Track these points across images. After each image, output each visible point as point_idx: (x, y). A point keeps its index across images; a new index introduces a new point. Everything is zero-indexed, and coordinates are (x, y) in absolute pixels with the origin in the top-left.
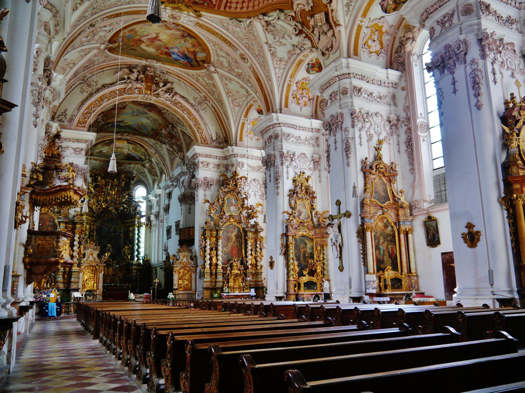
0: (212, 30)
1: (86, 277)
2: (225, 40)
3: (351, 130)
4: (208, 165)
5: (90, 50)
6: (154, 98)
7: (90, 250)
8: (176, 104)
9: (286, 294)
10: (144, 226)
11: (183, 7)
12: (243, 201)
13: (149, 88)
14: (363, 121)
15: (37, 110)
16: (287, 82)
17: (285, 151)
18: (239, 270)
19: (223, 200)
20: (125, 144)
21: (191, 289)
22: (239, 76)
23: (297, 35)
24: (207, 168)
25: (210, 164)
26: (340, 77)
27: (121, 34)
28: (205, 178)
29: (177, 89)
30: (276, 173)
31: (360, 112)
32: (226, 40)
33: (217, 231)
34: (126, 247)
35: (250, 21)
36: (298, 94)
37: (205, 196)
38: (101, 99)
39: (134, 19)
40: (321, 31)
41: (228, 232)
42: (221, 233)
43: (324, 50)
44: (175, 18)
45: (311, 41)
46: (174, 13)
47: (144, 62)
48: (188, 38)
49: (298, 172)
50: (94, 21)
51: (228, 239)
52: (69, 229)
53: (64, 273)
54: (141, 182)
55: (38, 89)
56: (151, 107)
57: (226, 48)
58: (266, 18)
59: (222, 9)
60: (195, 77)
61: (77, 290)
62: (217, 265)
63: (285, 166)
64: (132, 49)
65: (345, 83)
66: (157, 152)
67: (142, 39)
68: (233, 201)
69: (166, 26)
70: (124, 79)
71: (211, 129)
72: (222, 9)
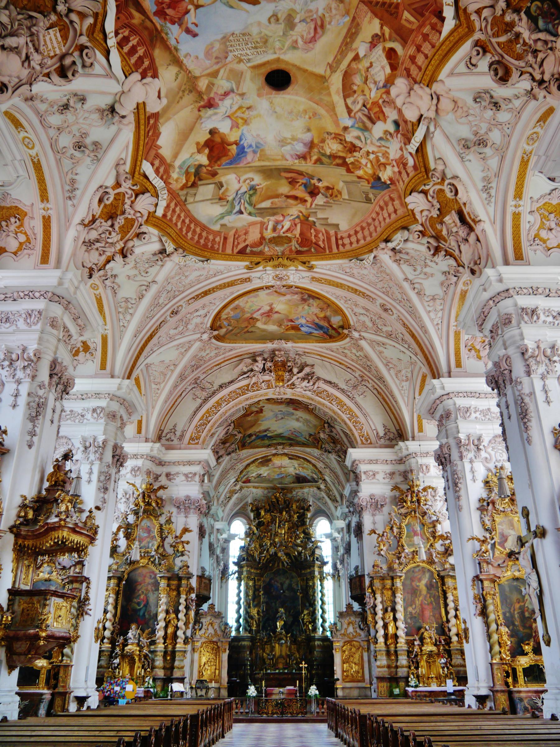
1: (204, 660)
2: (355, 291)
3: (525, 380)
4: (374, 475)
5: (190, 344)
6: (289, 391)
7: (209, 618)
8: (318, 393)
9: (493, 691)
10: (329, 578)
11: (285, 262)
12: (434, 526)
13: (279, 379)
14: (547, 361)
15: (34, 426)
16: (452, 329)
17: (462, 436)
18: (435, 645)
19: (400, 528)
20: (285, 461)
21: (363, 680)
22: (389, 336)
23: (434, 255)
24: (374, 481)
25: (378, 473)
26: (496, 298)
27: (224, 316)
28: (372, 497)
29: (319, 372)
30: (454, 473)
31: (538, 347)
32: (356, 290)
33: (392, 578)
34: (306, 612)
35: (372, 255)
36: (476, 344)
37: (374, 523)
38: (219, 404)
39: (232, 293)
40: (460, 239)
41: (412, 580)
42: (398, 583)
43: (471, 265)
44: (281, 279)
45: (455, 258)
47: (269, 346)
48: (311, 301)
49: (491, 466)
50: (175, 307)
51: (413, 592)
52: (173, 587)
53: (165, 653)
54: (321, 513)
55: (37, 399)
56: (293, 403)
57: (361, 301)
59: (335, 250)
60: (341, 350)
61: (181, 680)
62: (396, 637)
63: (466, 461)
64: (248, 332)
65: (506, 306)
66: (327, 466)
67: (254, 316)
68: (418, 528)
70: (245, 373)
71: (375, 421)
72: (335, 250)
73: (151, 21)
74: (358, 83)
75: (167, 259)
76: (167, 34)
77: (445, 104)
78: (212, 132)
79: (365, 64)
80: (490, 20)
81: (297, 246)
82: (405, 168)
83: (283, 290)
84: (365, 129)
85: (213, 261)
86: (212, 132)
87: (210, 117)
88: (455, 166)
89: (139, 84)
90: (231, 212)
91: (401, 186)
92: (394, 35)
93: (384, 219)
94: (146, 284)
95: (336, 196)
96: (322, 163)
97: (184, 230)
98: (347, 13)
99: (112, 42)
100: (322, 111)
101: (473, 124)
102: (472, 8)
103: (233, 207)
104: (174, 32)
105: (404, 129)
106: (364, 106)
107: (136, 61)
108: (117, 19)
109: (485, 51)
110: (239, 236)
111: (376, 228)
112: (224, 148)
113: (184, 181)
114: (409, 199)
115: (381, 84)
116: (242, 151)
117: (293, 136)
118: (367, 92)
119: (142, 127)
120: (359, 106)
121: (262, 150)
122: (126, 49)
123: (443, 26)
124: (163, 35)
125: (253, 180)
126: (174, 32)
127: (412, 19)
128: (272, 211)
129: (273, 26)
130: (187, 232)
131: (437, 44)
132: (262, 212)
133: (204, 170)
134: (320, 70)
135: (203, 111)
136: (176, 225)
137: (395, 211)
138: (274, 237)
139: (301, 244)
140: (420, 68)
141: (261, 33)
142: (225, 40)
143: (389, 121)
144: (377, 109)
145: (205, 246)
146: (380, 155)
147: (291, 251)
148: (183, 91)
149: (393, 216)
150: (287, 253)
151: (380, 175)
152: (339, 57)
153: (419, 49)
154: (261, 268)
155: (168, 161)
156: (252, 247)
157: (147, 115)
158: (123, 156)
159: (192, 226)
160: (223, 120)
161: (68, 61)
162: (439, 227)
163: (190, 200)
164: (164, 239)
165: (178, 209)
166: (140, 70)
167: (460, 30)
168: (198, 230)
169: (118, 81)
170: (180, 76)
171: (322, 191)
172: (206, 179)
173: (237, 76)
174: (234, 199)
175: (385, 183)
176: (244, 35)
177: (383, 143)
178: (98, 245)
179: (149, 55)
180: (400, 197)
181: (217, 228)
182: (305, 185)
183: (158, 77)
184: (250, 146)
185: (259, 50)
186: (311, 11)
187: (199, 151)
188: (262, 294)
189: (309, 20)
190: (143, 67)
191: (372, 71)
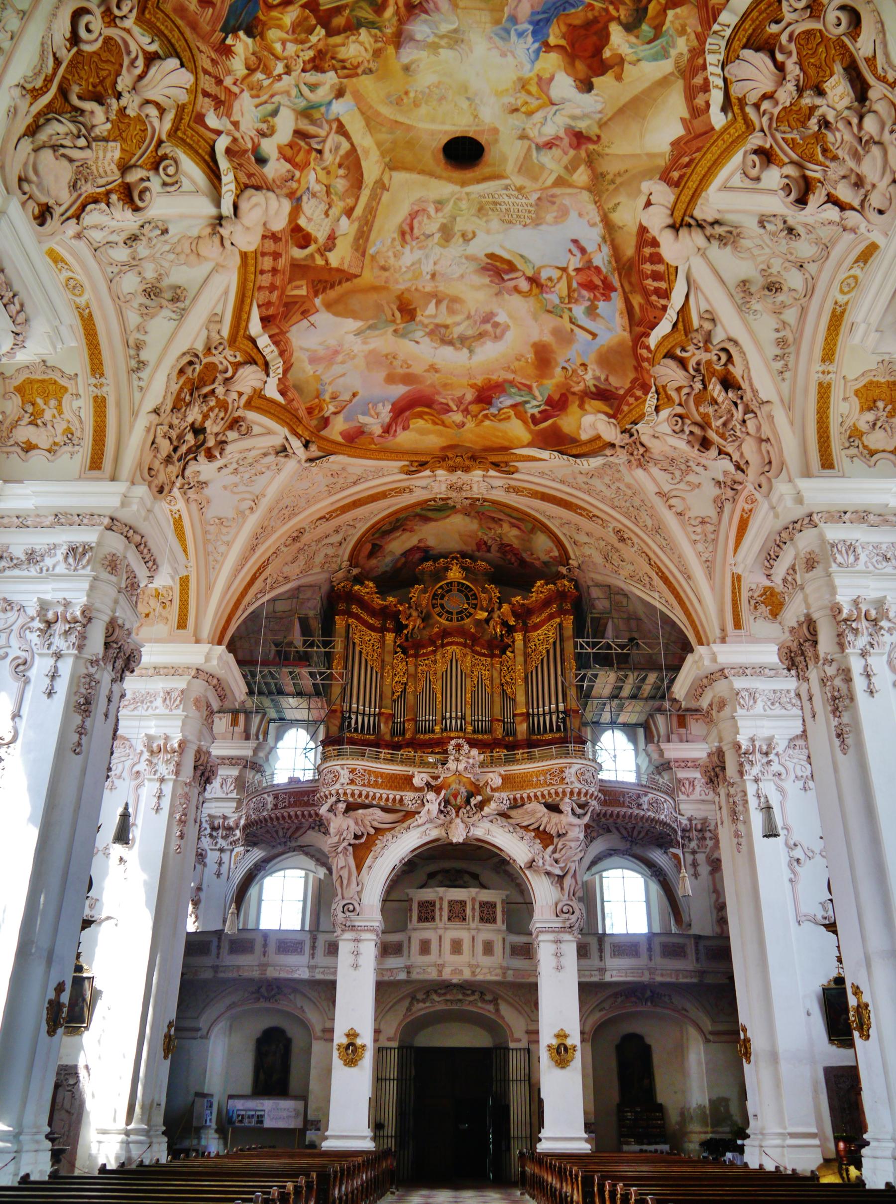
73: (622, 286)
74: (338, 180)
76: (610, 262)
78: (587, 86)
87: (585, 116)
92: (309, 262)
98: (373, 257)
99: (671, 315)
100: (387, 111)
106: (320, 152)
112: (572, 44)
113: (671, 13)
115: (305, 198)
118: (322, 175)
121: (497, 22)
126: (601, 258)
129: (469, 228)
131: (256, 294)
133: (623, 13)
134: (399, 177)
135: (595, 131)
141: (487, 222)
142: (537, 222)
144: (298, 159)
146: (266, 83)
151: (250, 41)
152: (374, 204)
155: (680, 84)
157: (677, 190)
170: (611, 205)
173: (526, 167)
175: (234, 31)
176: (510, 222)
177: (269, 107)
184: (520, 35)
185: (491, 200)
186: (420, 248)
189: (422, 237)
191: (323, 207)
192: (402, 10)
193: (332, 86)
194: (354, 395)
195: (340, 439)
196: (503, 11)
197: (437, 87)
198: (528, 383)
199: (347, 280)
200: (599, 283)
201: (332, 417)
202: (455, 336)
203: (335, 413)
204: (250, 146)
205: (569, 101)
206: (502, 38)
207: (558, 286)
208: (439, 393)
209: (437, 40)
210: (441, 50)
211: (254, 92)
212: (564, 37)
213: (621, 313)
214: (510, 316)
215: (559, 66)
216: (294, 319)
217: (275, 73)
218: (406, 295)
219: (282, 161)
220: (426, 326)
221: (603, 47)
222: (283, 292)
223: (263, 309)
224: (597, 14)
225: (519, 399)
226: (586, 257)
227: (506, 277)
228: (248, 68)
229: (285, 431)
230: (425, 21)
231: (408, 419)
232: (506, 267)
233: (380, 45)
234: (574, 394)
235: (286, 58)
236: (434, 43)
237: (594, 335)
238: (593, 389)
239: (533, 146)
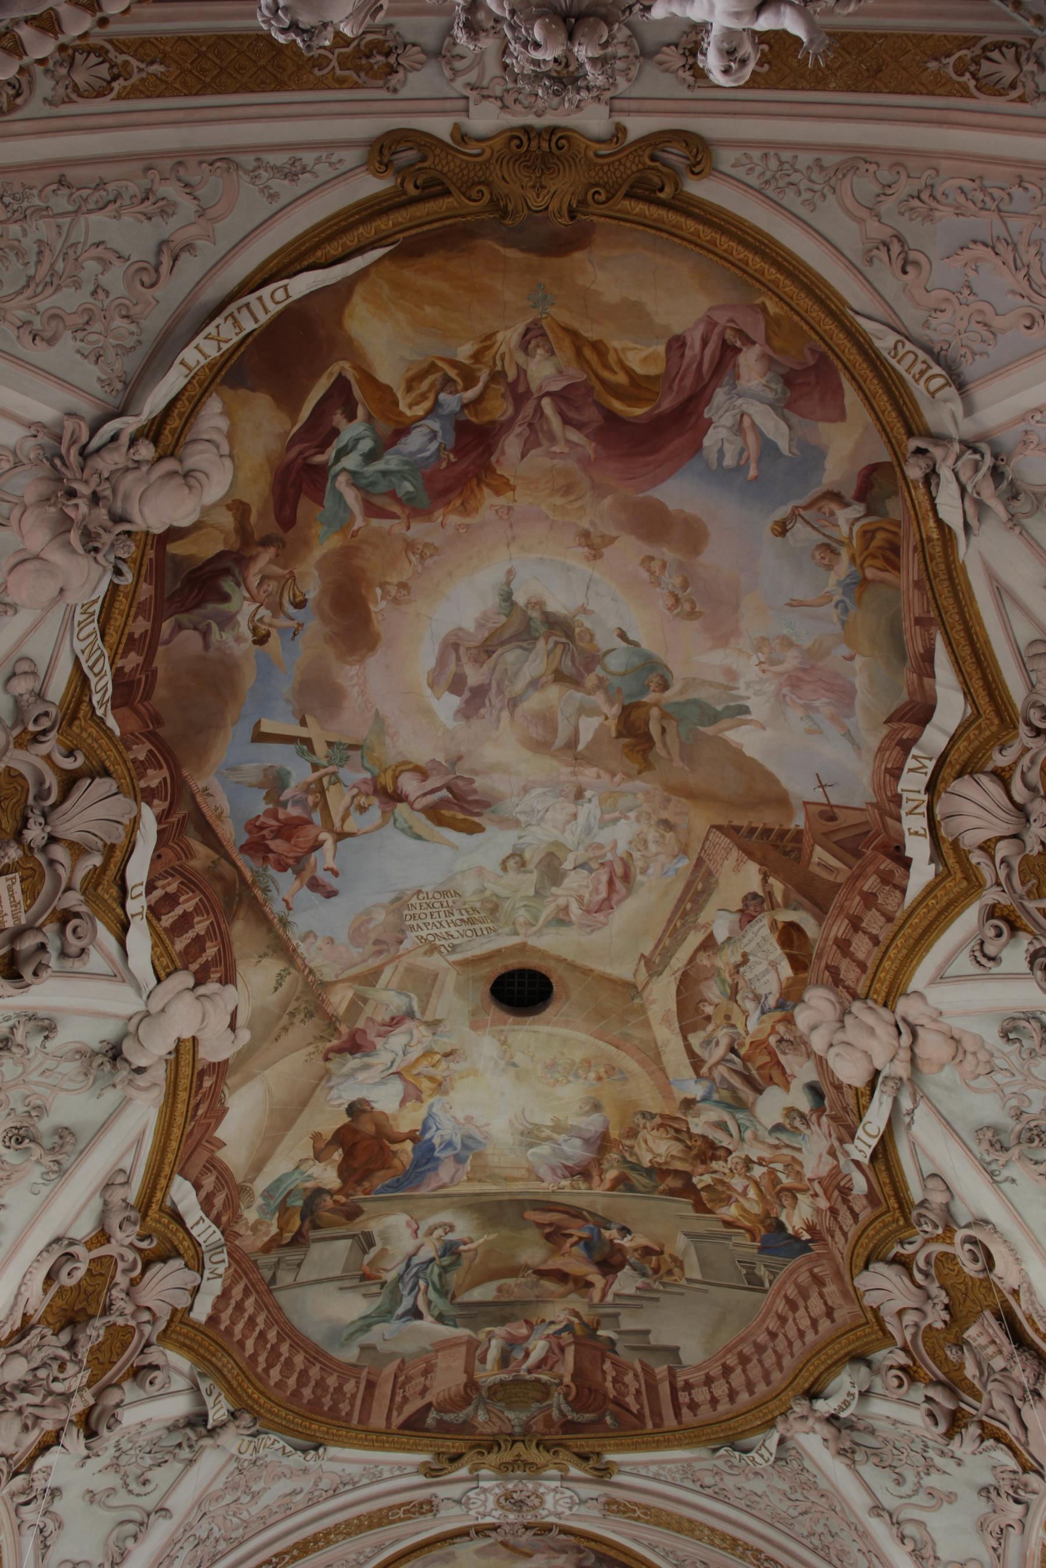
0: (669, 1514)
11: (534, 1455)
32: (735, 1540)
39: (380, 1548)
40: (1017, 1392)
44: (519, 1505)
46: (510, 1486)
58: (824, 1407)
59: (670, 1422)
69: (504, 1544)
72: (670, 1422)
73: (234, 864)
74: (716, 1000)
75: (207, 1442)
76: (266, 890)
77: (931, 1046)
79: (730, 957)
80: (1015, 863)
81: (565, 1408)
82: (845, 1201)
83: (526, 1538)
84: (737, 1105)
85: (333, 1451)
86: (355, 1109)
87: (351, 1074)
88: (975, 1194)
89: (189, 997)
90: (390, 1312)
91: (840, 1246)
92: (795, 896)
93: (801, 1334)
94: (137, 1515)
95: (670, 1272)
96: (631, 1188)
97: (262, 1359)
98: (684, 851)
99: (137, 905)
100: (630, 1064)
101: (1008, 1090)
102: (971, 840)
103: (396, 1298)
104: (283, 887)
105: (836, 1105)
107: (188, 946)
108: (157, 857)
109: (1014, 928)
110: (409, 1379)
111: (779, 1357)
112: (383, 1148)
113: (274, 1230)
114: (864, 1280)
115: (772, 1002)
116: (426, 1157)
117: (555, 1120)
118: (737, 1019)
119: (183, 1095)
120: (720, 1051)
121: (478, 1155)
122: (167, 920)
123: (908, 877)
124: (258, 892)
125: (452, 1228)
126: (283, 887)
127: (834, 862)
128: (500, 1311)
129: (513, 877)
130: (270, 1365)
132: (474, 1314)
133: (329, 1202)
134: (623, 971)
135: (336, 1059)
136: (241, 1344)
137: (829, 1313)
138: (502, 1383)
139: (577, 1404)
140: (862, 966)
141: (483, 890)
142: (400, 903)
143: (797, 1086)
144: (766, 1059)
145: (315, 1405)
147: (548, 1421)
148: (292, 1015)
149: (824, 1325)
150: (538, 1427)
151: (783, 1218)
152: (667, 942)
153: (856, 924)
154: (463, 1472)
155: (239, 1179)
156: (441, 1409)
157: (199, 1067)
158: (126, 1164)
159: (285, 1348)
160: (383, 1081)
161: (27, 944)
162: (952, 1355)
163: (286, 1278)
164: (204, 1385)
165: (250, 1303)
166: (194, 967)
167: (948, 884)
168: (299, 1360)
169: (138, 989)
170: (288, 979)
171: (632, 1258)
172: (332, 1224)
173: (426, 983)
174: (400, 1278)
175: (796, 1238)
176: (444, 893)
177: (785, 1138)
178: (25, 1399)
179: (219, 934)
180: (838, 1275)
181: (350, 1355)
182: (588, 1244)
183: (235, 984)
184: (449, 1144)
185: (477, 927)
186: (600, 846)
187: (319, 1156)
188: (465, 1550)
189: (594, 865)
190: (202, 960)
191: (749, 973)
192: (595, 1173)
193: (697, 1115)
194: (782, 529)
195: (851, 396)
196: (472, 1166)
197: (557, 1081)
198: (375, 522)
199: (737, 829)
200: (272, 844)
201: (849, 491)
202: (541, 644)
203: (835, 496)
204: (824, 1119)
205: (375, 1084)
206: (471, 1137)
207: (347, 799)
208: (585, 463)
209: (555, 1136)
210: (550, 1123)
211: (797, 1168)
212: (394, 1153)
213: (219, 817)
214: (429, 713)
215: (395, 1120)
216: (854, 818)
217: (765, 1169)
218: (636, 767)
219: (788, 1071)
220: (601, 684)
221: (344, 1160)
222: (855, 878)
223: (897, 880)
224: (360, 1189)
225: (391, 461)
226: (307, 876)
227: (444, 793)
228: (795, 1198)
229: (966, 552)
230: (568, 1158)
231: (667, 378)
232: (446, 812)
233: (628, 1142)
234: (266, 542)
235: (749, 1178)
236: (559, 1133)
237: (260, 737)
238: (227, 585)
239: (418, 1015)
